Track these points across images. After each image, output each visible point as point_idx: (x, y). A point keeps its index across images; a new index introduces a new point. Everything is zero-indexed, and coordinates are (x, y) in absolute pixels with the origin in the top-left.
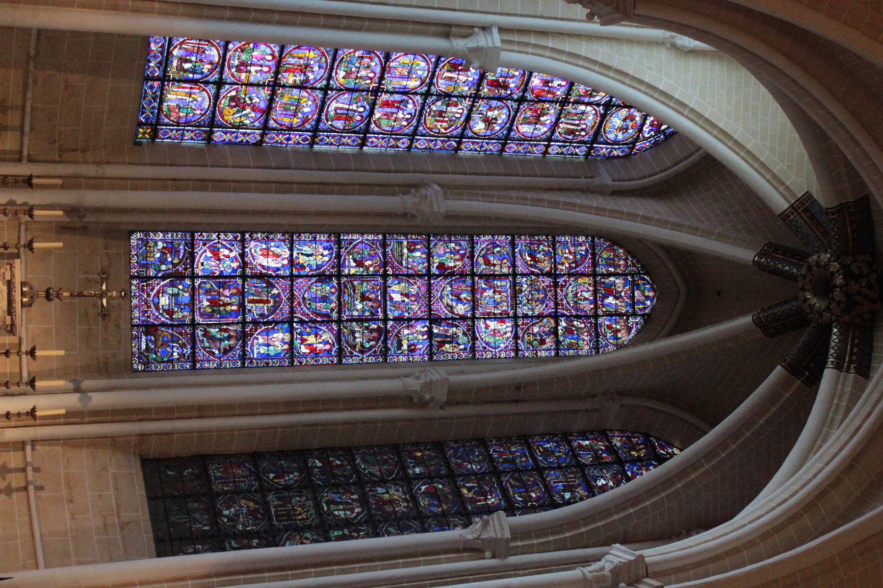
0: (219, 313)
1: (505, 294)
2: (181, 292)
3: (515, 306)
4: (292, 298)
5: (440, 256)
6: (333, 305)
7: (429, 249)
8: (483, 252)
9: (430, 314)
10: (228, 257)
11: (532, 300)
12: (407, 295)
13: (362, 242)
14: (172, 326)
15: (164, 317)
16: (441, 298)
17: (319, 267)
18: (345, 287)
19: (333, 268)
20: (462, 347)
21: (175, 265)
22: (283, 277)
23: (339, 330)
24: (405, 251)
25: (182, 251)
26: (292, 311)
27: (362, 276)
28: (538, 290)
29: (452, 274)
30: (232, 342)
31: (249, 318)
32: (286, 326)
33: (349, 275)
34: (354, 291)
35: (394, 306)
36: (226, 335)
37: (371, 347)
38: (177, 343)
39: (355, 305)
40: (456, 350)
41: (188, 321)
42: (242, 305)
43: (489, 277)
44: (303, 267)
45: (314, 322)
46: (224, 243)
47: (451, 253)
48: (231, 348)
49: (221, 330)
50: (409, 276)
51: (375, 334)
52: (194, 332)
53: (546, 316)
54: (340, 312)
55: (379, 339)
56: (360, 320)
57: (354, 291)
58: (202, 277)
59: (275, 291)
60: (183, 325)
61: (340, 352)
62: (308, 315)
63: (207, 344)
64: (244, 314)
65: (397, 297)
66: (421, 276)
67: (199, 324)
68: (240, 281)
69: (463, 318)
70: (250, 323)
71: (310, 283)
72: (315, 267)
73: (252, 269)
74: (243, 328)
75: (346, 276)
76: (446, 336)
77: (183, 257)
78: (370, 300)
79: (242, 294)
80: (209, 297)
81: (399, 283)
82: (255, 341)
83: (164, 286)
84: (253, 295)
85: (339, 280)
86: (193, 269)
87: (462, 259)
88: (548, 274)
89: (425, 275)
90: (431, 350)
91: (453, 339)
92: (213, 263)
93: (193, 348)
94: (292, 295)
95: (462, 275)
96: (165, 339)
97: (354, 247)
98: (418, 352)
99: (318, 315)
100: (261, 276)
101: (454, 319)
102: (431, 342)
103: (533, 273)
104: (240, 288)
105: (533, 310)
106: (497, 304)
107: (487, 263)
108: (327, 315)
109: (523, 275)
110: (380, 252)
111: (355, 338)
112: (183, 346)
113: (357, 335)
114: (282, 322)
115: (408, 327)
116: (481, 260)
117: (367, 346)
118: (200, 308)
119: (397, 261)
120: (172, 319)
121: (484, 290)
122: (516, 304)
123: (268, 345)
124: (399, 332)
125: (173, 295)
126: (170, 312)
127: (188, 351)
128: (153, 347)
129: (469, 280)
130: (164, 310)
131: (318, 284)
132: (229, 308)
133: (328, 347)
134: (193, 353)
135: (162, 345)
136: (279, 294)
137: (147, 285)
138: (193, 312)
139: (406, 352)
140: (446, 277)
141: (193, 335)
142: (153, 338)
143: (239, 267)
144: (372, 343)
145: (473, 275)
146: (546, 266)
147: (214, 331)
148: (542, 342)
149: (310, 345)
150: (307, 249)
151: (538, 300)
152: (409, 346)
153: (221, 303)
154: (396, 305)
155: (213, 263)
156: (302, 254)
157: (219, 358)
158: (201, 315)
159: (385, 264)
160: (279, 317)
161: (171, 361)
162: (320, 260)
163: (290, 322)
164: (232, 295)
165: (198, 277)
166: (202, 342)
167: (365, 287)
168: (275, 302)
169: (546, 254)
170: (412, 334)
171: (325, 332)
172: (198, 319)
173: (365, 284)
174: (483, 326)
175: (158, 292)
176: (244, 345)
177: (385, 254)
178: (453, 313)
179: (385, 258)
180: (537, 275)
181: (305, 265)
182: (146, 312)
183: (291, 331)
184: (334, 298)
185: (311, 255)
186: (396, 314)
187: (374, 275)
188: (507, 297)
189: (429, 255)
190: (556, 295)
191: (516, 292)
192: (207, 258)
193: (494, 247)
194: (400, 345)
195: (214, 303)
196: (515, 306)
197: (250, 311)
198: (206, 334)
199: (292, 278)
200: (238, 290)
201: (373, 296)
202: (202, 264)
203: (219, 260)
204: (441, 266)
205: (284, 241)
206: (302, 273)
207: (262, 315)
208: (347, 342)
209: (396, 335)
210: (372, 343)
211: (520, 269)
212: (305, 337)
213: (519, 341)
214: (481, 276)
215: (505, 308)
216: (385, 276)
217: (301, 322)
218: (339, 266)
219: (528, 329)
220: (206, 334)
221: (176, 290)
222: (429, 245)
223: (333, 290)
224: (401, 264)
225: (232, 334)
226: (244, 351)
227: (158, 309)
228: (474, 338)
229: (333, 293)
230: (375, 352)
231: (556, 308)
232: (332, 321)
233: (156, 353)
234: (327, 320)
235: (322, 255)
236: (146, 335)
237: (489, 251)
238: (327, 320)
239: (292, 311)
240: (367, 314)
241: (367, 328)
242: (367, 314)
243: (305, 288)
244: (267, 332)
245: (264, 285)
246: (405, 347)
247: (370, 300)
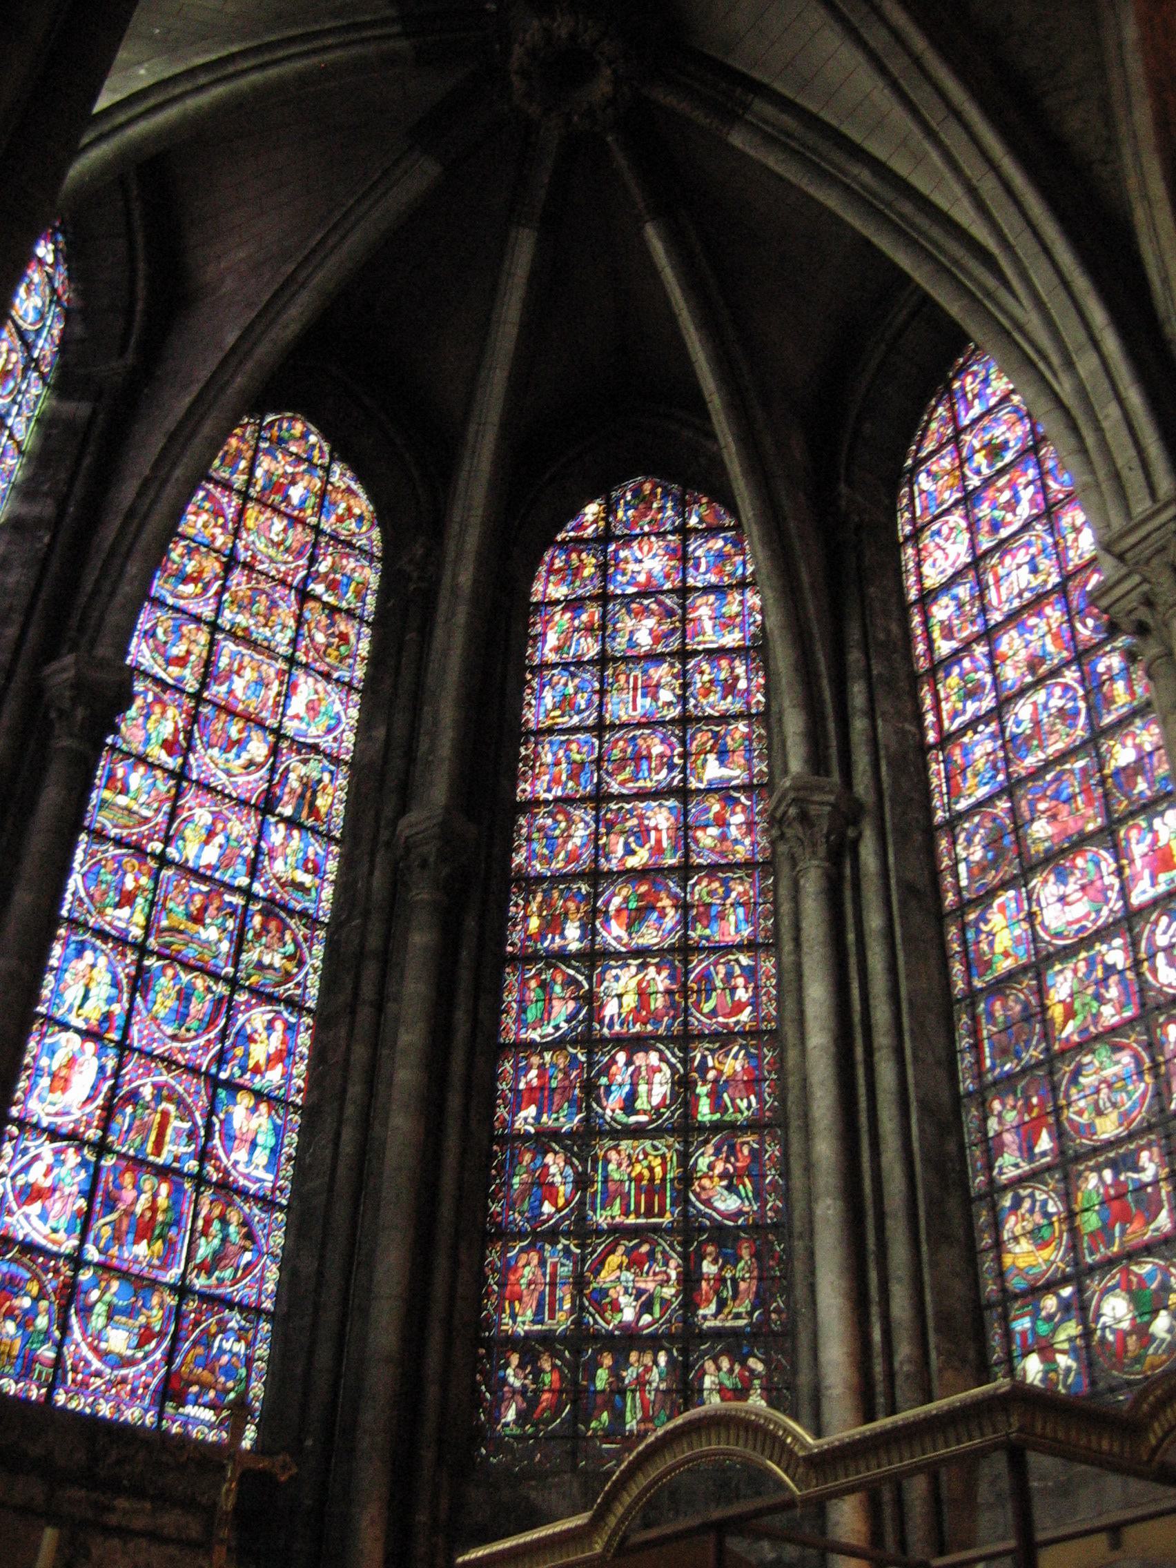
0: (167, 1225)
1: (247, 659)
2: (107, 1297)
3: (269, 651)
4: (169, 1063)
5: (147, 741)
6: (199, 983)
7: (128, 755)
8: (160, 660)
9: (256, 807)
10: (50, 1169)
11: (267, 618)
12: (211, 834)
13: (84, 876)
14: (176, 1339)
15: (154, 1351)
16: (228, 773)
17: (116, 983)
18: (168, 945)
19: (124, 955)
20: (326, 777)
21: (42, 1295)
22: (120, 1066)
23: (254, 991)
24: (122, 800)
25: (14, 1267)
26: (193, 1070)
27: (152, 904)
28: (252, 602)
29: (189, 736)
30: (234, 1217)
31: (192, 1165)
32: (222, 1093)
33: (147, 929)
34: (181, 932)
35: (228, 866)
36: (216, 1225)
37: (295, 940)
38: (215, 1336)
39: (208, 942)
40: (330, 790)
41: (172, 1301)
42: (163, 1172)
43: (209, 672)
44: (107, 1017)
45: (223, 1036)
46: (16, 1167)
47: (147, 717)
48: (245, 1222)
49: (205, 1233)
50: (173, 815)
51: (273, 925)
52: (197, 1292)
53: (301, 609)
54: (216, 977)
55: (282, 920)
56: (239, 944)
57: (181, 932)
58: (83, 1239)
59: (147, 1092)
60: (178, 1315)
61: (291, 1003)
62: (209, 1041)
63: (228, 1273)
64: (178, 1172)
65: (211, 855)
66: (179, 794)
67: (183, 1276)
68: (108, 1162)
69: (275, 751)
70: (202, 1167)
71: (144, 1013)
72: (114, 992)
73: (88, 1125)
74: (209, 1183)
75: (147, 935)
76: (302, 796)
77: (28, 1269)
78: (204, 909)
79: (138, 1164)
80: (130, 1237)
81: (184, 839)
82: (241, 1167)
83: (84, 1333)
84: (144, 1141)
85: (152, 953)
86: (56, 1256)
87: (164, 706)
88: (228, 568)
89: (178, 786)
90: (319, 833)
91: (310, 788)
92: (58, 1206)
93: (228, 1303)
94: (162, 1058)
95: (194, 718)
96: (201, 1360)
97: (91, 897)
98: (320, 859)
99: (212, 1023)
100: (109, 1112)
101: (273, 770)
102: (308, 829)
103: (219, 594)
104: (124, 1163)
105: (284, 627)
106: (262, 683)
107: (181, 661)
108: (218, 1002)
109: (218, 611)
110: (113, 851)
111: (271, 966)
112: (222, 1327)
113: (267, 960)
114: (213, 1098)
115: (272, 859)
116: (175, 671)
117: (290, 948)
118: (149, 1265)
119: (140, 824)
120: (161, 1335)
121: (230, 692)
122: (268, 648)
123: (254, 1145)
124: (278, 879)
125: (110, 1318)
126: (146, 1334)
127: (235, 1320)
128: (212, 1394)
129: (206, 710)
130: (139, 1346)
131: (150, 997)
132: (162, 1202)
133: (279, 1025)
134: (243, 1308)
135: (212, 1372)
136: (155, 1085)
137: (75, 1370)
138: (154, 1284)
139: (318, 881)
140: (190, 748)
141: (205, 1297)
142: (195, 1389)
143: (79, 1150)
144: (288, 937)
145: (197, 697)
146: (212, 566)
147: (205, 1249)
148: (344, 638)
149: (269, 1059)
150: (73, 994)
151: (270, 609)
152: (307, 871)
153: (148, 1214)
154: (226, 860)
155: (58, 1206)
156: (80, 1007)
157: (261, 1255)
158: (166, 1264)
159: (139, 851)
160: (203, 1101)
161: (249, 1361)
162: (102, 976)
163: (214, 1083)
164: (136, 1186)
165: (80, 1248)
166: (221, 1282)
167: (177, 908)
168: (169, 1099)
169: (190, 552)
170: (286, 857)
171: (248, 1020)
172: (172, 1275)
173: (170, 905)
174: (296, 723)
175: (95, 1350)
176: (243, 1193)
177: (119, 842)
178: (262, 765)
179: (128, 846)
180: (224, 589)
181: (105, 1009)
182: (134, 1390)
183: (233, 1087)
184: (185, 978)
185: (87, 991)
186: (241, 868)
187: (155, 876)
188: (252, 659)
189: (142, 759)
190: (267, 575)
191: (245, 639)
192: (44, 1217)
193: (154, 635)
194: (300, 887)
195: (144, 1230)
196: (269, 651)
197: (177, 1159)
198: (207, 1268)
199: (123, 1047)
200: (127, 1169)
201: (198, 900)
202: (55, 1231)
203: (53, 1189)
204: (169, 746)
205: (43, 1035)
206: (120, 1022)
207: (192, 1135)
208: (278, 985)
209: (283, 885)
210: (288, 937)
211: (207, 612)
212: (251, 1064)
213: (335, 675)
214: (204, 686)
215: (272, 672)
216: (163, 860)
217: (221, 1059)
218: (121, 941)
219: (317, 651)
220: (207, 1268)
221: (100, 1308)
222: (120, 751)
223: (170, 972)
224: (147, 820)
225: (217, 1212)
226: (258, 1198)
227: (131, 1362)
228: (315, 748)
229: (176, 976)
230: (306, 940)
231: (290, 587)
232: (231, 999)
233: (228, 1392)
234: (224, 1006)
235: (93, 966)
236: (183, 1404)
237: (160, 649)
238: (224, 1006)
239: (193, 1070)
240: (230, 924)
241: (258, 936)
242: (230, 924)
243: (154, 1028)
244: (229, 1138)
245: (129, 1109)
246: (307, 879)
247: (204, 909)
